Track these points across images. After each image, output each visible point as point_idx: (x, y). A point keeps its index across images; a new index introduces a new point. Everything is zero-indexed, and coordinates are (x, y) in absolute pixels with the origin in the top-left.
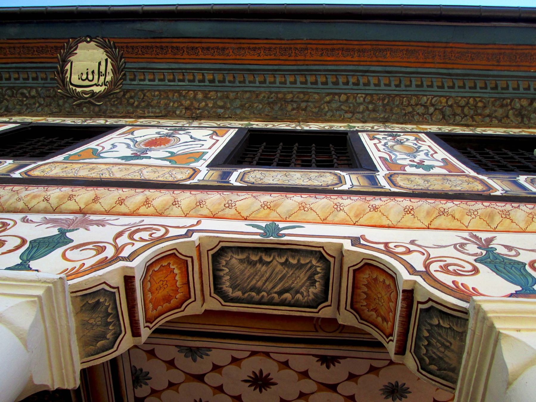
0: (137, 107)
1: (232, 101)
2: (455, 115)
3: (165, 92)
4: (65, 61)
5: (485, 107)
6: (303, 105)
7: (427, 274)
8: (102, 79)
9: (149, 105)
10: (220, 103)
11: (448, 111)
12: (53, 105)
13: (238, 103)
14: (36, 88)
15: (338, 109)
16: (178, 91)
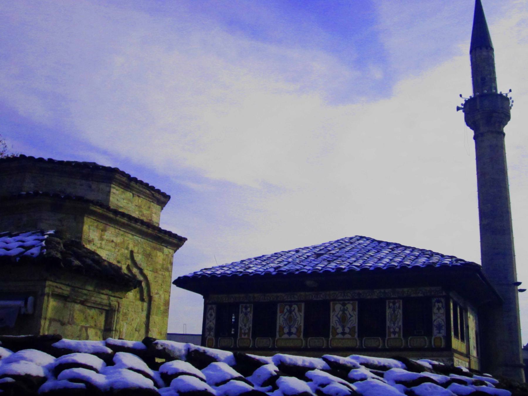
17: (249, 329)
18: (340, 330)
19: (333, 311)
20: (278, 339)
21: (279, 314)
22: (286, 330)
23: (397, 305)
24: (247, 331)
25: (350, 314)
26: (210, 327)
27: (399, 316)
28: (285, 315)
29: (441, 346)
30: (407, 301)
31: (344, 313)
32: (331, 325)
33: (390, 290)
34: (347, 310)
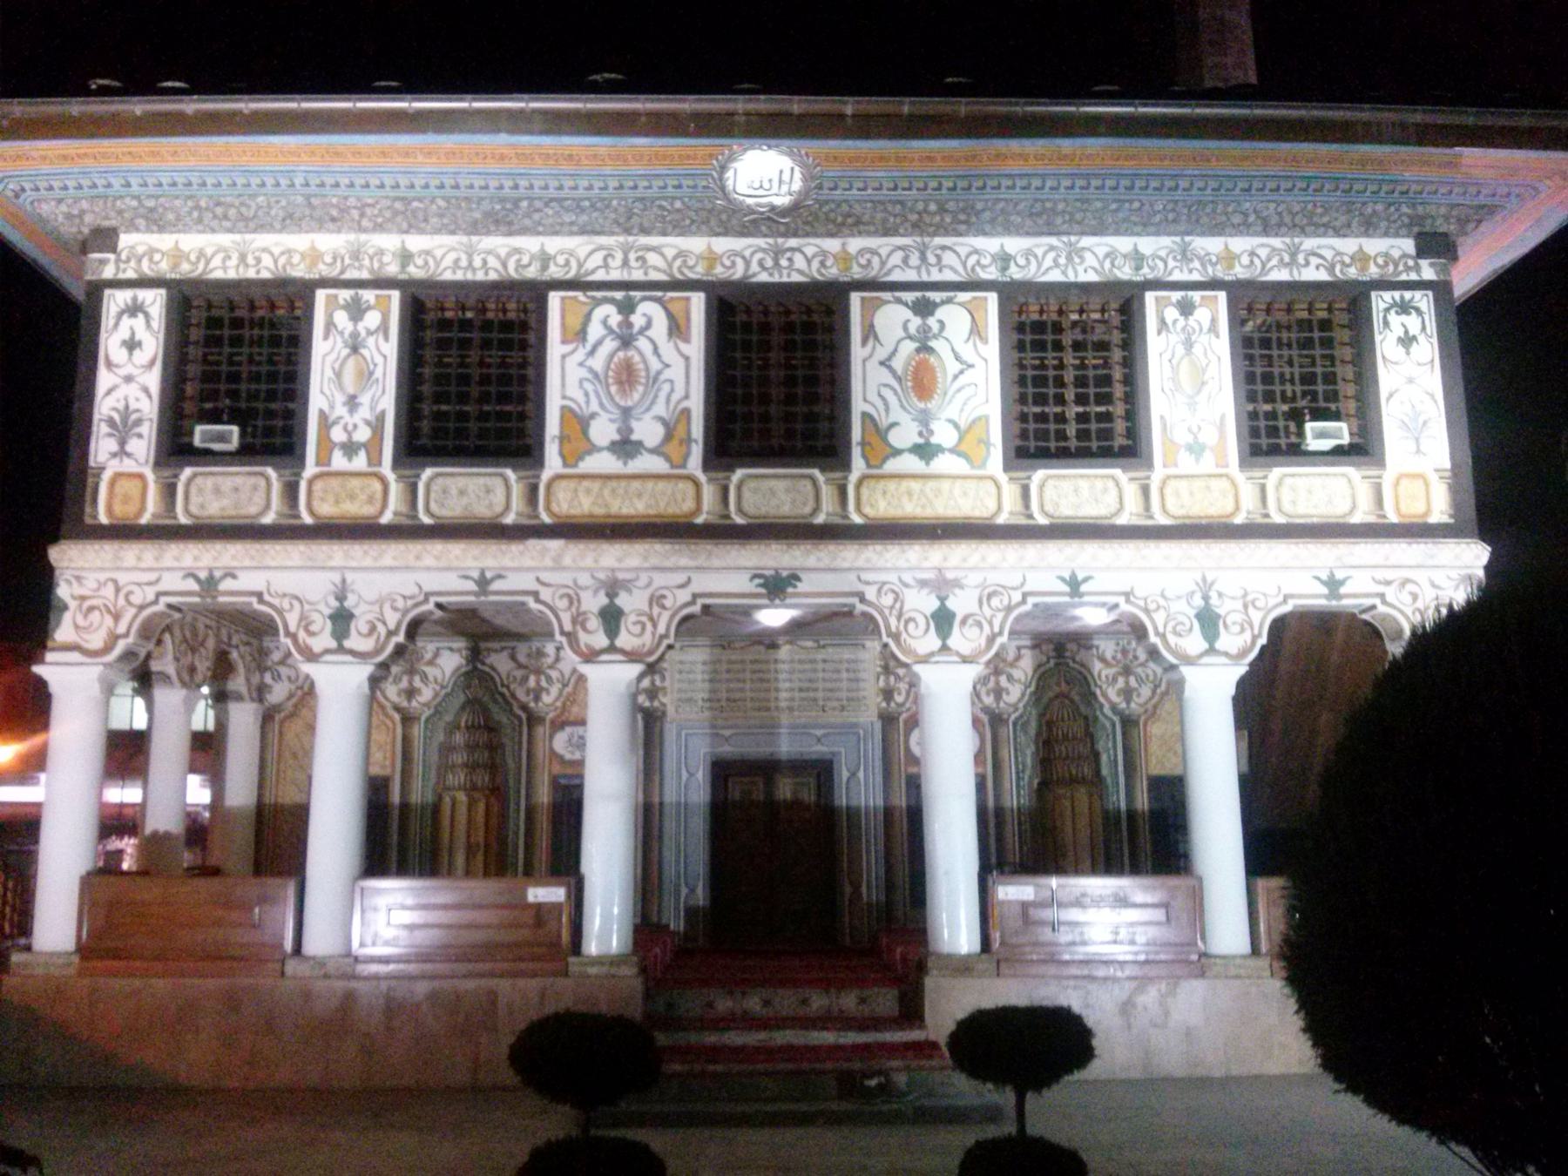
0: (843, 224)
1: (978, 213)
2: (1279, 225)
3: (882, 203)
4: (723, 168)
5: (1322, 215)
6: (1078, 216)
7: (1163, 637)
8: (785, 188)
9: (858, 222)
10: (962, 217)
11: (1274, 220)
12: (713, 222)
13: (987, 215)
14: (680, 199)
15: (1125, 220)
16: (901, 203)
17: (377, 426)
18: (905, 434)
19: (864, 342)
20: (559, 477)
21: (555, 347)
22: (603, 431)
23: (1202, 315)
24: (363, 434)
25: (957, 358)
26: (126, 412)
27: (1212, 371)
28: (592, 352)
29: (1428, 513)
30: (1250, 301)
31: (924, 348)
32: (858, 406)
33: (1166, 241)
34: (935, 337)
